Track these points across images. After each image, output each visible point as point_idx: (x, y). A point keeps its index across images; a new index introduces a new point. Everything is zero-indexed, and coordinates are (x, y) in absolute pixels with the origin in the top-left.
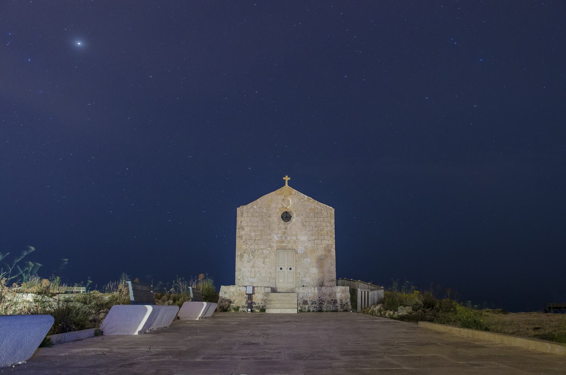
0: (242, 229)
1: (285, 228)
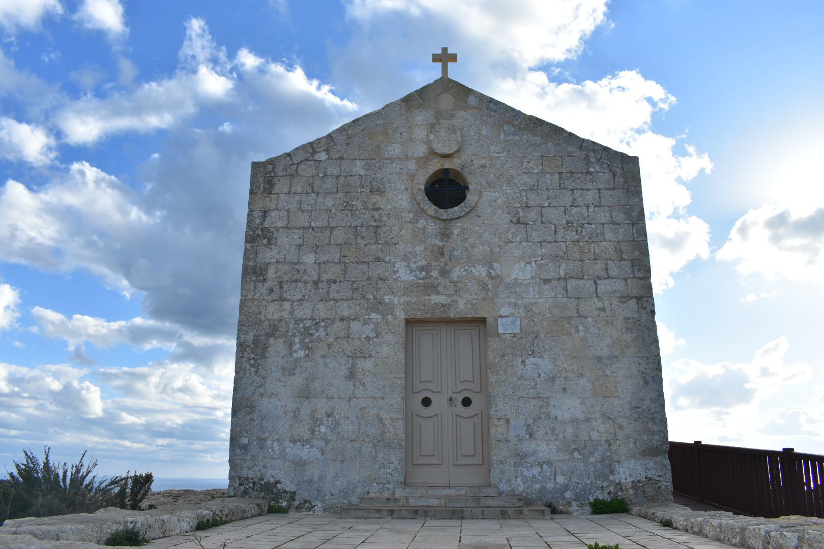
0: (265, 241)
1: (443, 234)
